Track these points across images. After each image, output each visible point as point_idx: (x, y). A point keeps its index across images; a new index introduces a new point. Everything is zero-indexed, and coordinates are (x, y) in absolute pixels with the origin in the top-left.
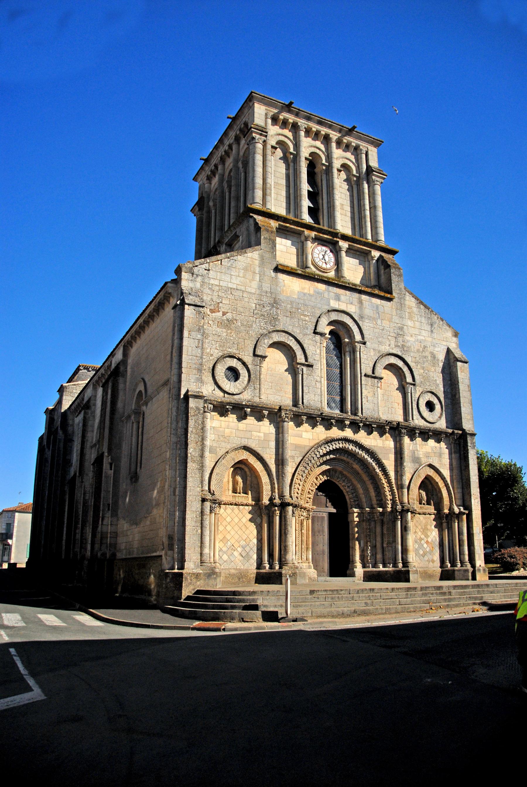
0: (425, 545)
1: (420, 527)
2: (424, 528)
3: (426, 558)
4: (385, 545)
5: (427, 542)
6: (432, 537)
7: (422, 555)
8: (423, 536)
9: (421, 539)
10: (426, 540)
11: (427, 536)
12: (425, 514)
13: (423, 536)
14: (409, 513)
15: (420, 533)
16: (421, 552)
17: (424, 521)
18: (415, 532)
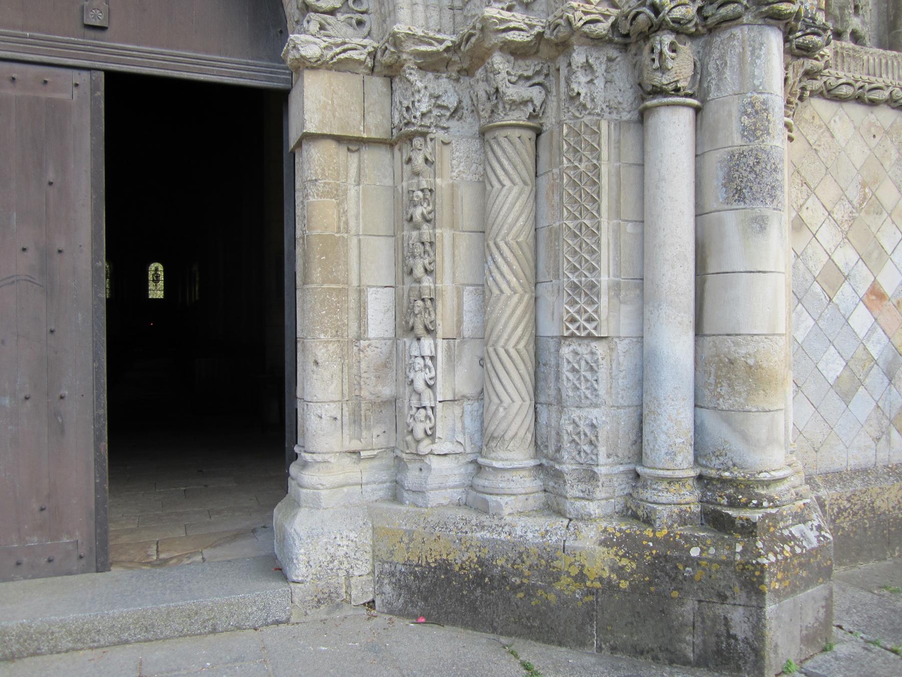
0: (861, 319)
1: (828, 192)
2: (854, 194)
3: (863, 405)
5: (876, 294)
7: (836, 386)
8: (846, 257)
9: (835, 277)
10: (863, 280)
11: (873, 255)
12: (873, 103)
13: (846, 257)
14: (774, 40)
15: (828, 235)
16: (833, 367)
17: (858, 153)
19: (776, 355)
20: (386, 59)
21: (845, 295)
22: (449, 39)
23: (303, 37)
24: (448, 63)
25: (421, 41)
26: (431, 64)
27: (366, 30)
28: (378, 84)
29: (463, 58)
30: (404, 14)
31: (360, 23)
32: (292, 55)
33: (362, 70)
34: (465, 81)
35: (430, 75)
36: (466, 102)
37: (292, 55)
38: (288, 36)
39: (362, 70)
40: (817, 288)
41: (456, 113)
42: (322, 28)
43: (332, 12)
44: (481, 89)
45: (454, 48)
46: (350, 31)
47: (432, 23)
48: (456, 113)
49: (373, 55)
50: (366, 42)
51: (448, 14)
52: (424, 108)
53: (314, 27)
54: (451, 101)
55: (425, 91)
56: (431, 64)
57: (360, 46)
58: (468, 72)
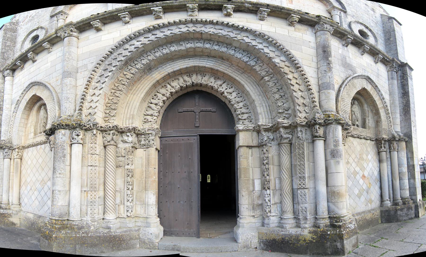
4: (295, 187)
6: (368, 169)
18: (348, 163)
19: (343, 190)
20: (257, 128)
21: (358, 177)
22: (271, 125)
23: (239, 125)
24: (271, 130)
25: (264, 126)
26: (267, 130)
27: (252, 122)
28: (255, 134)
29: (274, 128)
30: (261, 120)
31: (251, 121)
32: (237, 129)
33: (251, 131)
34: (275, 133)
35: (267, 132)
36: (275, 137)
37: (237, 129)
38: (235, 126)
39: (251, 131)
40: (352, 175)
41: (273, 140)
42: (243, 123)
43: (245, 120)
44: (278, 135)
45: (272, 127)
46: (249, 123)
47: (267, 122)
48: (273, 140)
49: (254, 128)
50: (252, 125)
51: (270, 120)
52: (266, 139)
53: (241, 123)
54: (272, 137)
55: (265, 136)
56: (267, 130)
57: (251, 126)
58: (276, 131)
